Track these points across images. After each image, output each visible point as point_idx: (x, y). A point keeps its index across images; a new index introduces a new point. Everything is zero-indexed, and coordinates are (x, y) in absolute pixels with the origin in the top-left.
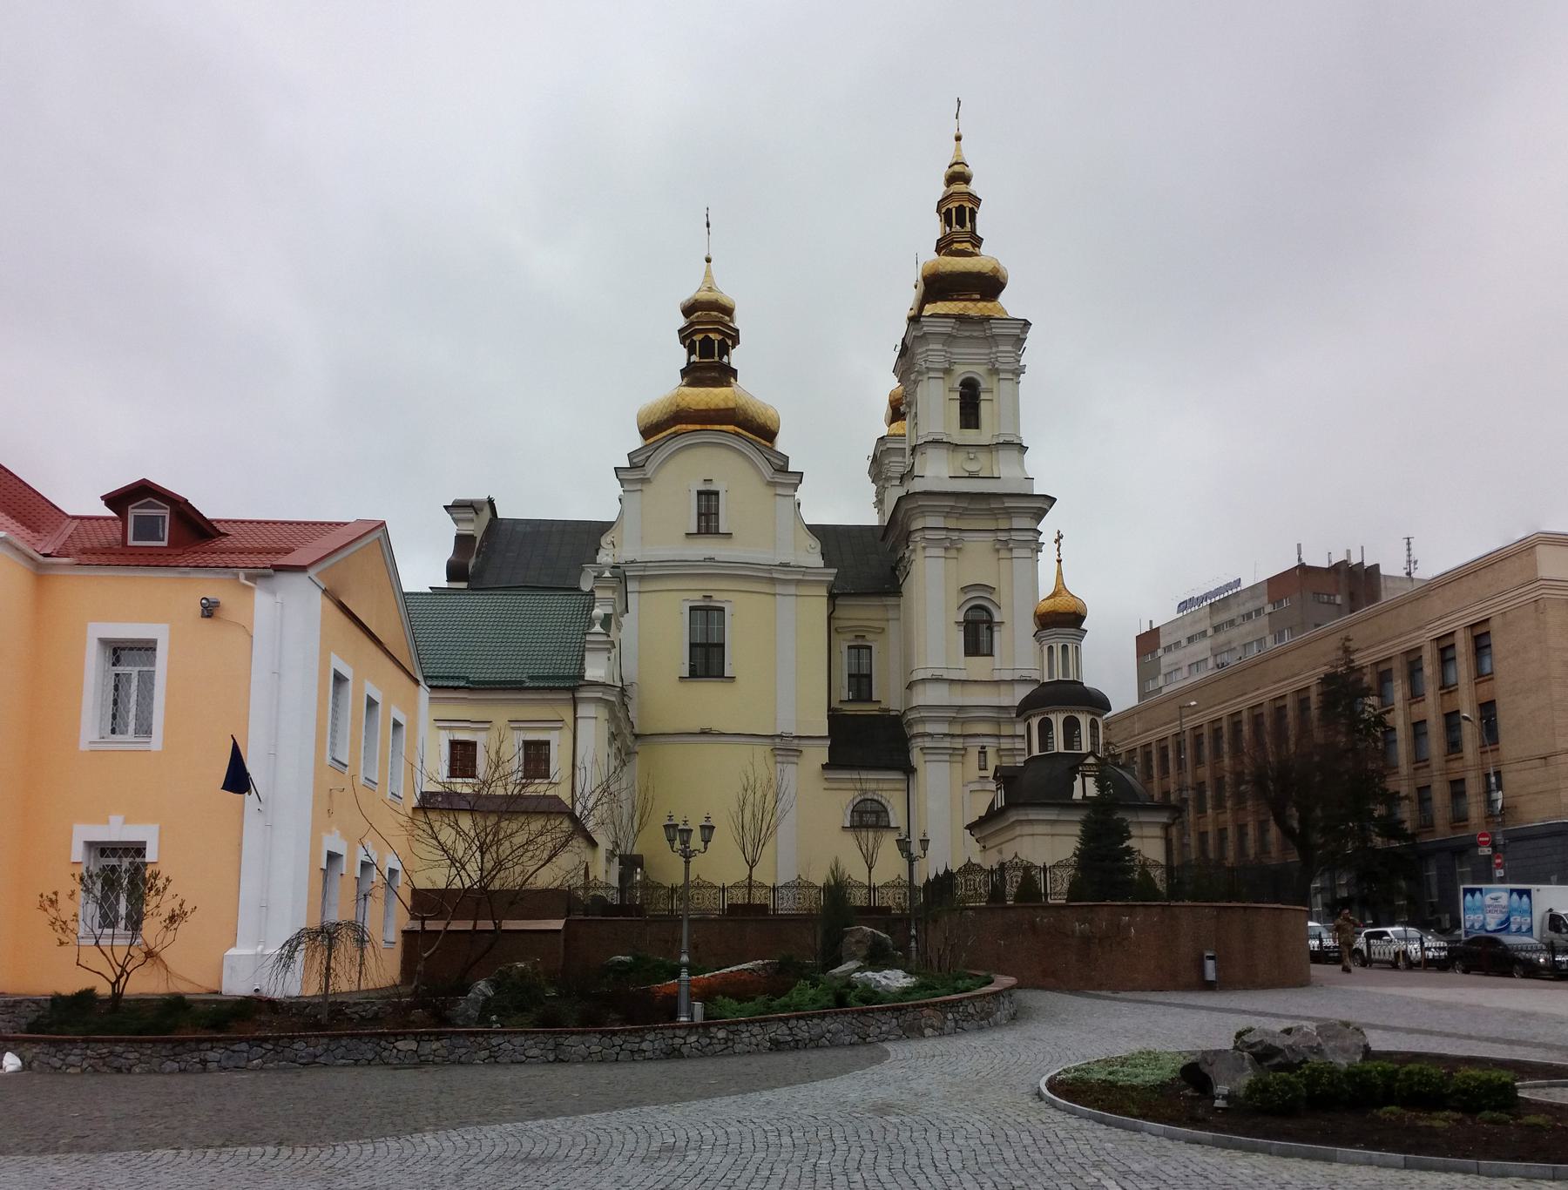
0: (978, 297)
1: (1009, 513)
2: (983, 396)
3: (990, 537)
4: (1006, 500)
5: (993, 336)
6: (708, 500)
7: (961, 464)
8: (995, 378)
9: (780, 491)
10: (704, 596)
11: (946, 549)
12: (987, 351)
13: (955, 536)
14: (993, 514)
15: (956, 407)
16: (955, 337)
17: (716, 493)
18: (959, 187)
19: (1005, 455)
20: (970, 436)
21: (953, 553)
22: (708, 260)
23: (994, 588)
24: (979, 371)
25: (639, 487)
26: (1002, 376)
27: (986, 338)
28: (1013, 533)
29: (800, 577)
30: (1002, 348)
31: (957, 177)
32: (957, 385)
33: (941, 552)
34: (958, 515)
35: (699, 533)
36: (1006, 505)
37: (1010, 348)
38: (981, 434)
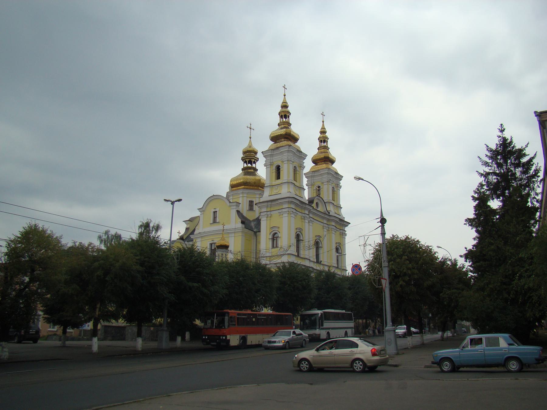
0: (283, 140)
1: (281, 204)
2: (281, 170)
4: (279, 200)
6: (215, 212)
9: (232, 208)
10: (212, 240)
11: (267, 217)
12: (281, 156)
13: (269, 213)
15: (274, 175)
16: (273, 154)
17: (217, 211)
18: (284, 109)
21: (269, 218)
22: (250, 138)
23: (279, 227)
24: (279, 163)
25: (203, 213)
28: (283, 209)
29: (234, 231)
30: (285, 155)
31: (285, 106)
32: (274, 167)
33: (265, 219)
35: (214, 223)
37: (287, 154)
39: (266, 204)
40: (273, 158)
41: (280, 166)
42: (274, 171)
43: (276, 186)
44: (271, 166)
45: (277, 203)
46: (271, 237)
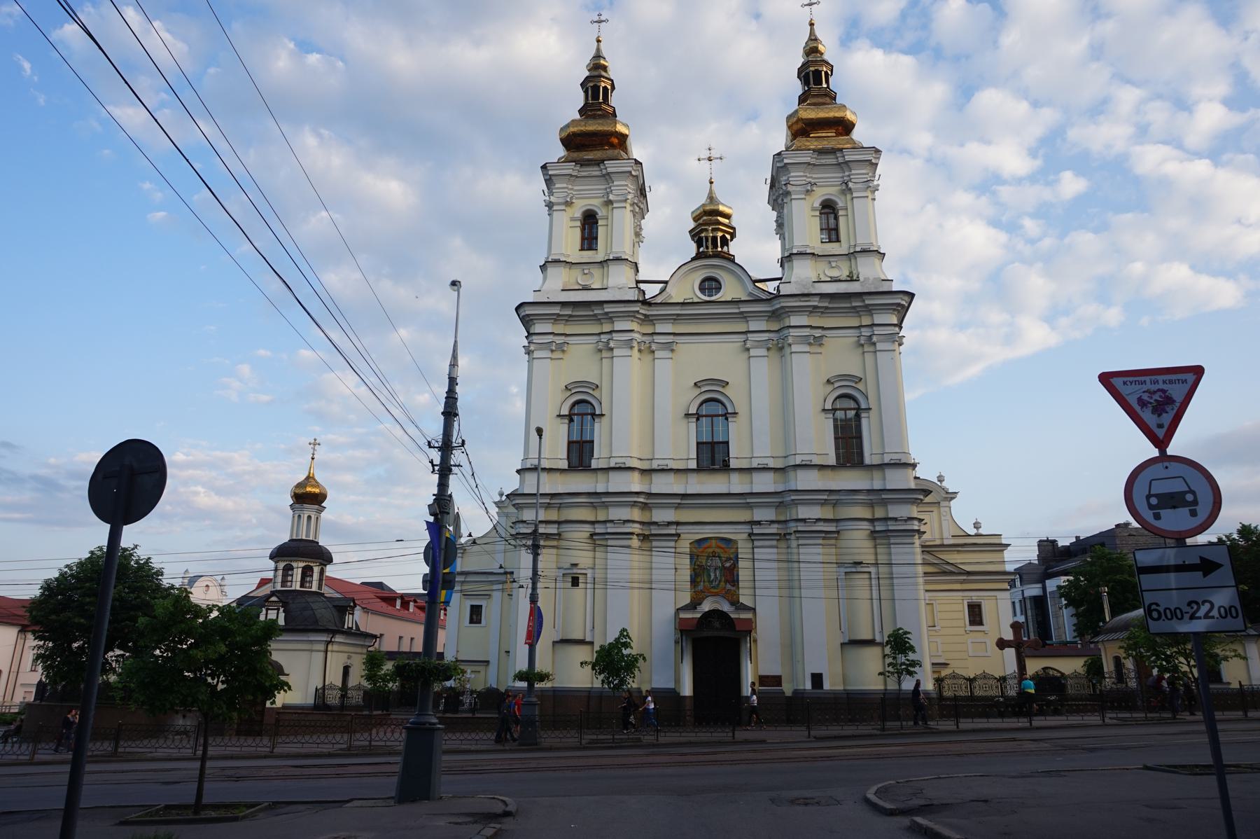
2: (600, 222)
3: (594, 339)
4: (605, 306)
5: (608, 174)
7: (576, 277)
8: (610, 207)
12: (604, 187)
14: (597, 319)
15: (577, 233)
19: (613, 269)
20: (588, 256)
21: (558, 355)
26: (615, 205)
27: (603, 176)
28: (614, 335)
31: (597, 67)
32: (578, 214)
34: (564, 322)
36: (606, 310)
38: (597, 254)
39: (556, 310)
40: (576, 188)
41: (597, 214)
42: (578, 224)
43: (585, 267)
44: (568, 209)
45: (595, 315)
46: (565, 411)
